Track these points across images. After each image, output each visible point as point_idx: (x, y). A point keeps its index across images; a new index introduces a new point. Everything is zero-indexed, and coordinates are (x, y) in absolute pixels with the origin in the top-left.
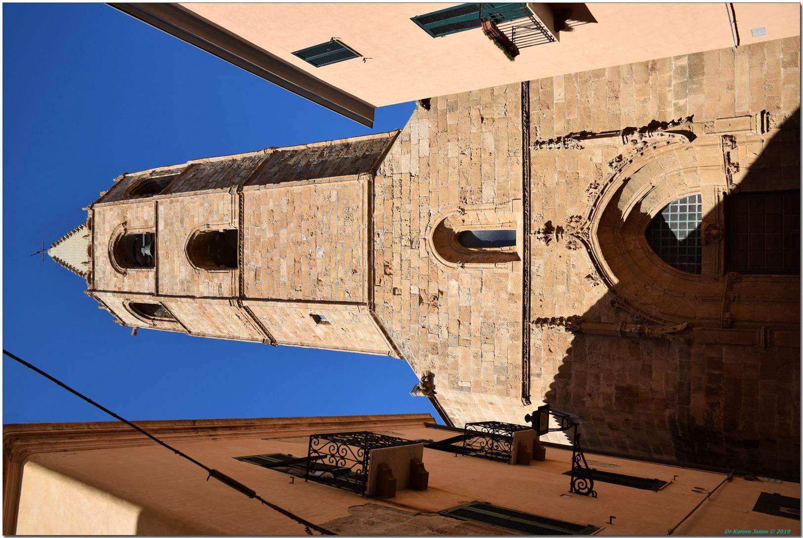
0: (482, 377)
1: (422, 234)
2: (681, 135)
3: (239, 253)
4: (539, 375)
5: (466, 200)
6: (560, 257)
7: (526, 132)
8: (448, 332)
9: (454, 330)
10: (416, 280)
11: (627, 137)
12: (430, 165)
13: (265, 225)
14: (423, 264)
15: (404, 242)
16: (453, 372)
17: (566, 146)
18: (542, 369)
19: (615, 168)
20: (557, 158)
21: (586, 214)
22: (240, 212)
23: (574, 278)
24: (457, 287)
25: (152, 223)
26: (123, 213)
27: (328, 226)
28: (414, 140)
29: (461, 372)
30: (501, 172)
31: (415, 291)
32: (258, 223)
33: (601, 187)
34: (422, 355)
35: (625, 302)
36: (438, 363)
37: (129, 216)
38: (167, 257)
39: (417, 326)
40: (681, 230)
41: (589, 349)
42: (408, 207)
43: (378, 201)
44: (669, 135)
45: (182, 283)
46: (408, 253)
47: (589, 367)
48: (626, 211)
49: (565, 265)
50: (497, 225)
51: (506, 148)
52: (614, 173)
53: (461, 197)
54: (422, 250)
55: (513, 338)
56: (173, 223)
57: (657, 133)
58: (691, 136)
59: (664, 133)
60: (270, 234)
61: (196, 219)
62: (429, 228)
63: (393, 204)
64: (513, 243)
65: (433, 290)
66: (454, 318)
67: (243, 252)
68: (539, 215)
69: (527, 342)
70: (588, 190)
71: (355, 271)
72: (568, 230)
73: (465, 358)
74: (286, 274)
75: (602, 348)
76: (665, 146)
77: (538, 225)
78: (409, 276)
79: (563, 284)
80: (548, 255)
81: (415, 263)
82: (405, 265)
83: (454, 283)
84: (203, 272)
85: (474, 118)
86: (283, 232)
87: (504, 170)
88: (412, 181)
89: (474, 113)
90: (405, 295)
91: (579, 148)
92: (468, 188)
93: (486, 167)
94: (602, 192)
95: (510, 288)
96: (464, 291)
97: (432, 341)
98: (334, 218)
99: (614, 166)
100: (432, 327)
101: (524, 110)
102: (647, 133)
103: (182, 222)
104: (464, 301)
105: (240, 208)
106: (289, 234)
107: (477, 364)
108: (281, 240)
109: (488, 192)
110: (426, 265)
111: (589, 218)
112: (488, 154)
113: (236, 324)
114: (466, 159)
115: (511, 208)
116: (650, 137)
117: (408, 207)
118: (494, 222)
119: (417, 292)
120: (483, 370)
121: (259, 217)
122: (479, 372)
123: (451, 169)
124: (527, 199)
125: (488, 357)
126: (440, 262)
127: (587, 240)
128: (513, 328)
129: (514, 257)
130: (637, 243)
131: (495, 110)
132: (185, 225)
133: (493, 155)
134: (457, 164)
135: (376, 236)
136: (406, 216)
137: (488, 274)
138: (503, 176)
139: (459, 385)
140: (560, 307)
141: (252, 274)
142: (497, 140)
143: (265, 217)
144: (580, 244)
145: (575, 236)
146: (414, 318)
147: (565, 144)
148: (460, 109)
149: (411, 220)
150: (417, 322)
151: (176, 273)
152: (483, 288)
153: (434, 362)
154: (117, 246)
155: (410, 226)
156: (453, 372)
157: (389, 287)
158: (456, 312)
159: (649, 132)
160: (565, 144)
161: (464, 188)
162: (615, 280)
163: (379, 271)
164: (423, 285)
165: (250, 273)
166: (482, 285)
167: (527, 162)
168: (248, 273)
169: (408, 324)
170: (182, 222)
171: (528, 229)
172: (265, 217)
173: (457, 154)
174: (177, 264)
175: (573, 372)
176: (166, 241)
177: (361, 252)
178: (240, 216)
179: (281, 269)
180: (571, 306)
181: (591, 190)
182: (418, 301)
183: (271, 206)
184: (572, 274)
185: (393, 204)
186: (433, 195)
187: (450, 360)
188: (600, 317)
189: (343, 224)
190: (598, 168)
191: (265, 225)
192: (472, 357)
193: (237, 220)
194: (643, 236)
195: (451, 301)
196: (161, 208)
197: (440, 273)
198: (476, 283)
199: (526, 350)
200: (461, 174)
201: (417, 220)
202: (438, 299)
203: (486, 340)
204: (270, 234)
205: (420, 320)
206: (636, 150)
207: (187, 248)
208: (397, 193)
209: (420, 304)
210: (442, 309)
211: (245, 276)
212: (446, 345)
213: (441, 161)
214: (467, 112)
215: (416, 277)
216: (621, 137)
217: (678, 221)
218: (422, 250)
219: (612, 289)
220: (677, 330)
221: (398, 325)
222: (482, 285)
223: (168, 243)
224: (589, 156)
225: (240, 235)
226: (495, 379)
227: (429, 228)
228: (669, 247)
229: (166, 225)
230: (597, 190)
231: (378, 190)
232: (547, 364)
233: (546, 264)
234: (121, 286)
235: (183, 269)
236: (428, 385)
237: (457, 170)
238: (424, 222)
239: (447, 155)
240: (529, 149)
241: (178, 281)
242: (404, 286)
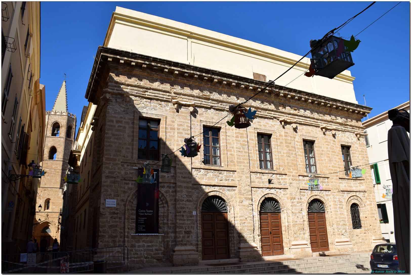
13: (55, 166)
26: (64, 126)
37: (63, 128)
38: (53, 140)
40: (47, 230)
42: (54, 194)
43: (55, 189)
45: (47, 144)
48: (49, 224)
58: (56, 232)
60: (53, 167)
61: (59, 149)
64: (47, 209)
65: (41, 198)
77: (49, 214)
83: (42, 201)
84: (49, 150)
93: (57, 206)
103: (59, 145)
109: (54, 207)
117: (54, 194)
121: (57, 165)
126: (45, 199)
129: (45, 210)
130: (46, 225)
141: (47, 163)
162: (40, 223)
163: (45, 189)
170: (59, 145)
191: (55, 166)
196: (62, 139)
204: (53, 167)
208: (56, 192)
211: (47, 161)
219: (39, 223)
229: (59, 140)
231: (57, 189)
235: (50, 145)
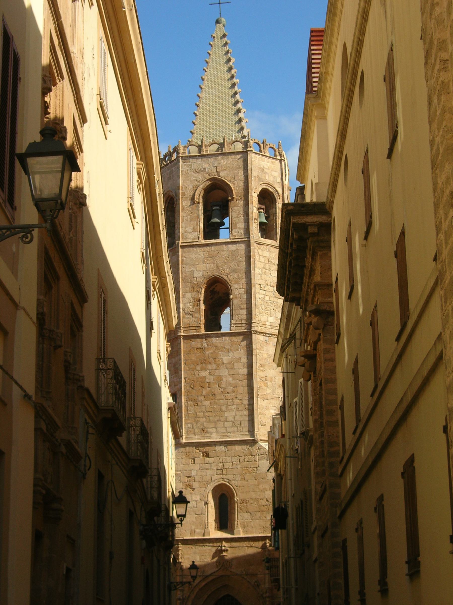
1: (225, 477)
14: (208, 478)
24: (196, 500)
31: (194, 473)
61: (236, 286)
62: (227, 481)
65: (195, 485)
78: (201, 469)
81: (209, 472)
83: (198, 498)
90: (192, 467)
92: (248, 505)
93: (259, 514)
98: (233, 413)
112: (265, 515)
117: (239, 467)
119: (193, 474)
123: (259, 493)
132: (232, 274)
133: (265, 518)
138: (254, 524)
141: (199, 346)
152: (196, 515)
164: (197, 478)
166: (198, 515)
173: (266, 497)
174: (203, 267)
207: (215, 277)
208: (247, 458)
234: (186, 196)
235: (200, 274)
237: (258, 497)
238: (230, 477)
241: (192, 269)
242: (197, 467)
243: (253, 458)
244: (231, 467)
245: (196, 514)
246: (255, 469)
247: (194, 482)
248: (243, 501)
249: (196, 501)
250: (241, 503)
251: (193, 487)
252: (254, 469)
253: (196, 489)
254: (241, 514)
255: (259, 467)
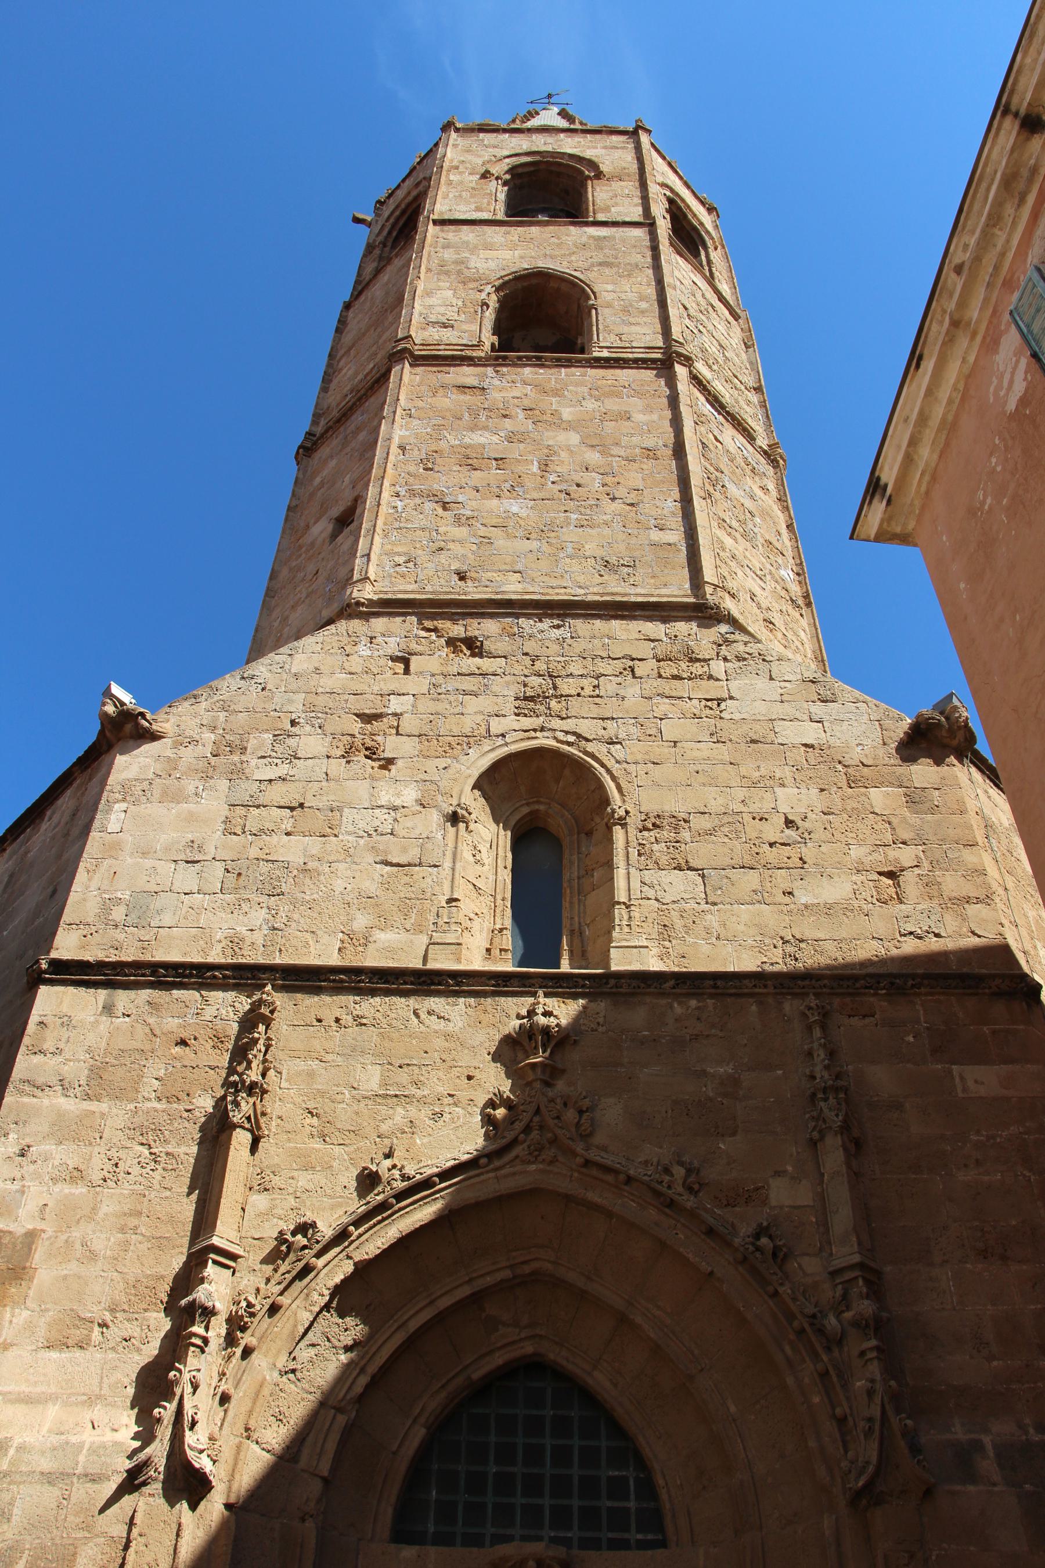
0: (129, 860)
1: (556, 723)
2: (874, 1459)
3: (525, 357)
4: (108, 1009)
5: (649, 830)
6: (470, 1078)
7: (858, 985)
8: (270, 781)
9: (277, 794)
10: (426, 705)
11: (856, 1278)
12: (752, 745)
15: (535, 681)
16: (157, 792)
17: (820, 1095)
18: (127, 1019)
19: (753, 1244)
20: (780, 1072)
21: (603, 1154)
22: (625, 361)
23: (400, 1115)
25: (601, 217)
27: (585, 523)
28: (818, 709)
29: (154, 810)
30: (734, 919)
32: (597, 393)
33: (689, 1202)
34: (216, 718)
35: (306, 1270)
36: (188, 754)
39: (297, 707)
41: (167, 1154)
44: (870, 1420)
46: (506, 691)
47: (113, 1153)
49: (442, 1090)
50: (576, 919)
51: (809, 934)
52: (737, 1241)
53: (658, 816)
54: (511, 722)
55: (235, 942)
56: (602, 249)
57: (878, 1377)
59: (878, 1399)
62: (571, 738)
63: (640, 660)
66: (309, 796)
67: (526, 365)
68: (601, 1020)
69: (215, 977)
70: (681, 1163)
71: (462, 577)
72: (552, 1100)
73: (191, 818)
74: (467, 440)
75: (168, 1193)
76: (833, 1408)
79: (384, 1084)
80: (476, 1043)
82: (468, 684)
83: (409, 795)
85: (892, 853)
86: (574, 438)
87: (741, 927)
88: (704, 702)
89: (906, 856)
91: (816, 1135)
92: (686, 835)
94: (671, 1204)
95: (383, 937)
96: (383, 819)
97: (252, 743)
99: (758, 1243)
100: (291, 742)
101: (926, 982)
102: (874, 1342)
104: (354, 820)
105: (636, 361)
106: (568, 449)
107: (167, 849)
108: (551, 434)
110: (467, 731)
111: (587, 1163)
112: (786, 886)
113: (356, 374)
114: (773, 830)
115: (626, 944)
116: (862, 1354)
118: (585, 912)
120: (148, 863)
121: (614, 393)
122: (144, 854)
123: (740, 793)
124: (649, 986)
125: (187, 878)
127: (517, 1157)
128: (260, 941)
131: (919, 907)
133: (787, 899)
134: (754, 807)
135: (556, 622)
136: (608, 686)
137: (429, 880)
139: (117, 806)
140: (311, 1074)
142: (829, 909)
143: (612, 405)
144: (506, 1134)
145: (531, 1121)
146: (321, 701)
147: (825, 1090)
148: (914, 819)
149: (597, 700)
150: (310, 708)
151: (483, 254)
152: (388, 868)
153: (191, 747)
154: (553, 168)
155: (579, 695)
156: (157, 792)
157: (414, 646)
158: (325, 798)
159: (878, 1348)
160: (824, 1093)
161: (686, 825)
164: (408, 724)
165: (473, 378)
166: (398, 865)
167: (765, 986)
168: (476, 373)
169: (305, 688)
171: (561, 987)
172: (612, 405)
173: (784, 808)
175: (104, 1106)
176: (559, 238)
177: (512, 588)
178: (617, 360)
179: (480, 432)
180: (311, 1105)
181: (679, 1172)
182: (367, 711)
183: (639, 417)
184: (413, 1112)
185: (640, 660)
186: (666, 750)
187: (191, 785)
188: (266, 1190)
189: (587, 554)
190: (754, 1196)
192: (190, 837)
193: (605, 354)
194: (529, 1348)
195: (361, 790)
197: (442, 763)
198: (404, 850)
199: (191, 976)
200: (726, 819)
201: (595, 712)
202: (367, 757)
203: (235, 872)
204: (567, 413)
205: (313, 714)
206: (810, 1310)
208: (669, 669)
209: (356, 715)
210: (337, 767)
211: (466, 369)
212: (236, 774)
213: (763, 771)
214: (905, 835)
215: (433, 707)
216: (856, 1258)
217: (575, 1472)
218: (511, 722)
220: (188, 1433)
221: (305, 666)
222: (398, 865)
223: (556, 241)
224: (790, 1168)
225: (569, 360)
226: (119, 895)
227: (571, 738)
228: (493, 1438)
230: (680, 1189)
232: (141, 1031)
233: (447, 1036)
236: (129, 727)
238: (585, 727)
239: (783, 785)
240: (807, 994)
242: (415, 684)
243: (698, 669)
244: (588, 691)
245: (387, 863)
246: (714, 704)
247: (394, 738)
248: (653, 823)
249: (395, 809)
250: (645, 829)
251: (388, 754)
252: (709, 704)
253: (400, 763)
254: (648, 876)
255: (731, 698)
